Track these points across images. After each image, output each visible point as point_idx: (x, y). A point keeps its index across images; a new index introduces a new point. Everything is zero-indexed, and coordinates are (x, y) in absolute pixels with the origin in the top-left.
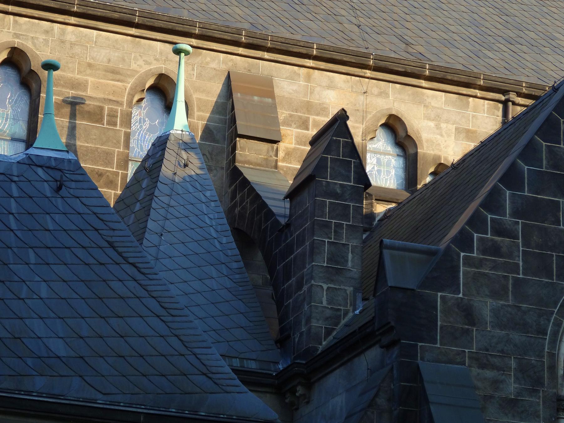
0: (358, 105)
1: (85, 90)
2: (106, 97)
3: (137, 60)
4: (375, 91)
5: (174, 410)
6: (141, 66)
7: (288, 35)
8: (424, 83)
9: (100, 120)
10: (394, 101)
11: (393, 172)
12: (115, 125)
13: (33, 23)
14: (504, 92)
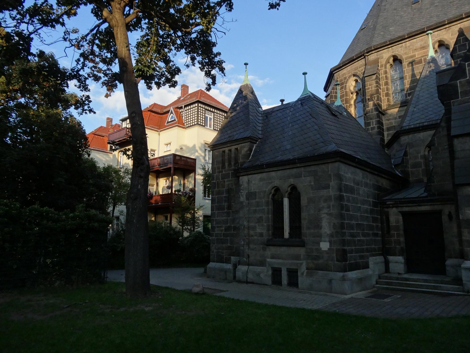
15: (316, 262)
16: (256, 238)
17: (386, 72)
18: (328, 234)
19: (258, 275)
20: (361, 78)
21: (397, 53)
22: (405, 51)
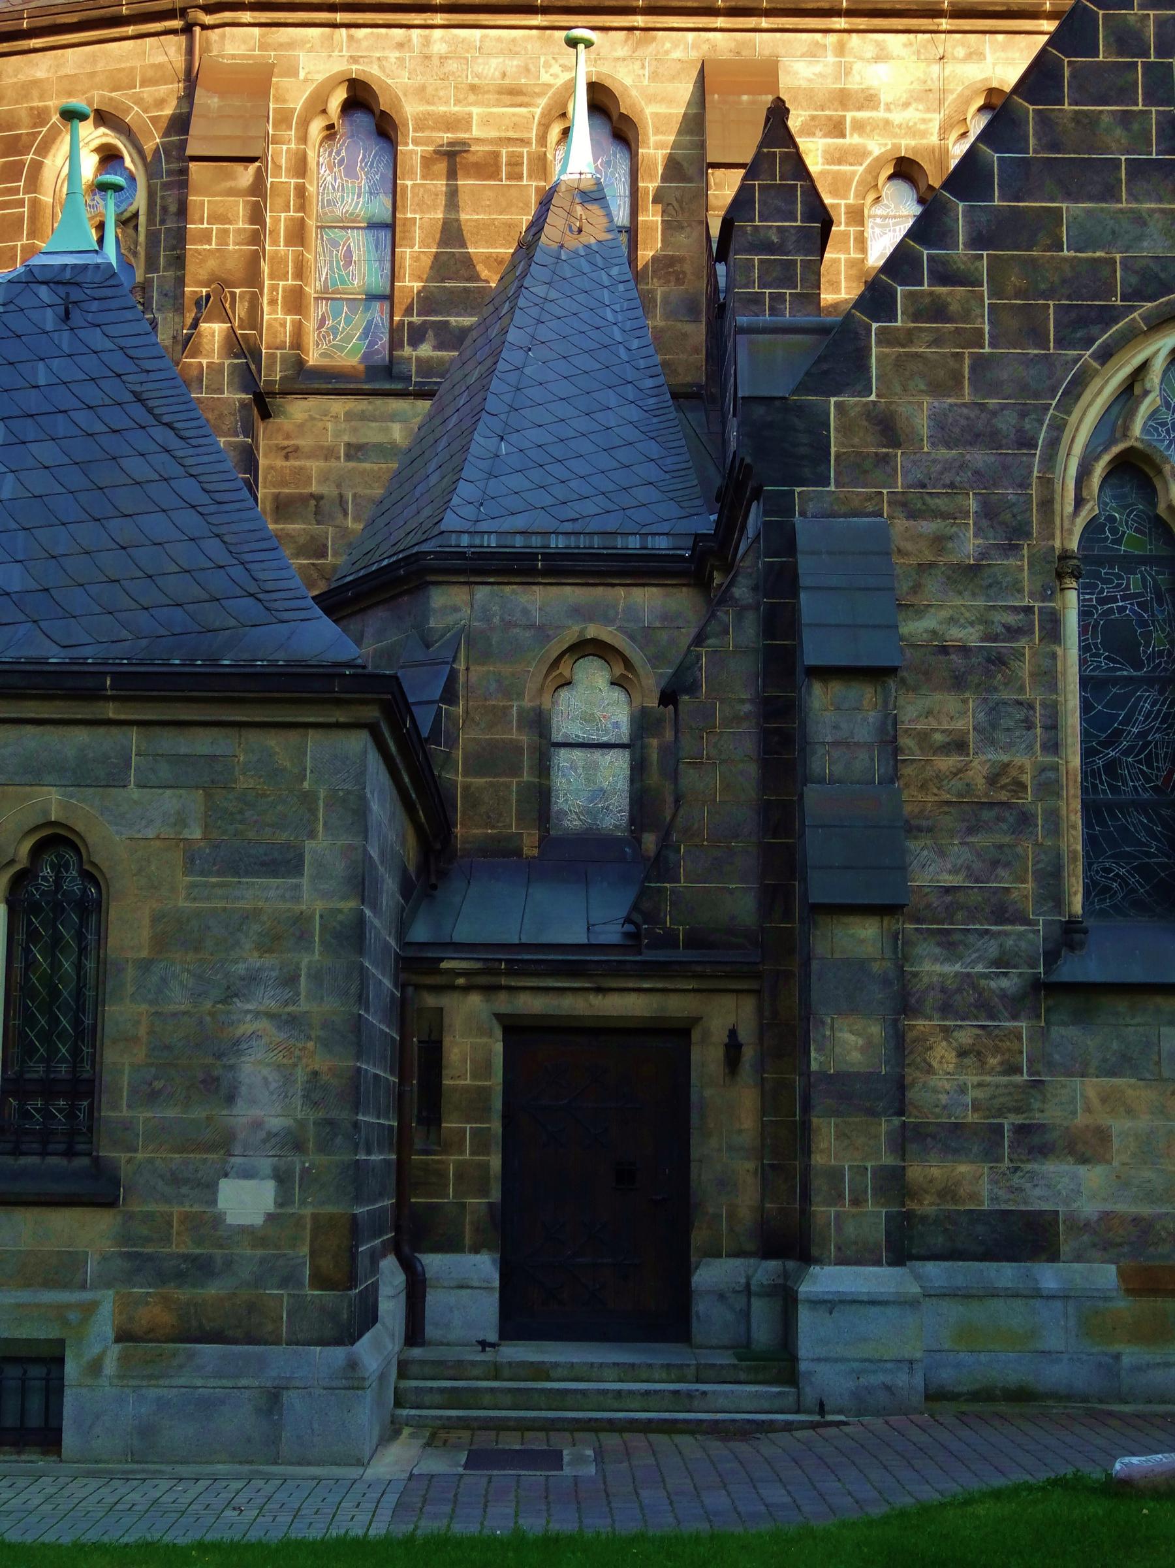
0: (929, 82)
1: (469, 128)
2: (503, 135)
3: (550, 66)
4: (960, 52)
5: (177, 662)
6: (555, 76)
9: (495, 174)
10: (994, 65)
12: (520, 178)
13: (379, 36)
15: (183, 1294)
17: (301, 167)
18: (271, 1135)
20: (149, 147)
21: (375, 70)
22: (420, 80)
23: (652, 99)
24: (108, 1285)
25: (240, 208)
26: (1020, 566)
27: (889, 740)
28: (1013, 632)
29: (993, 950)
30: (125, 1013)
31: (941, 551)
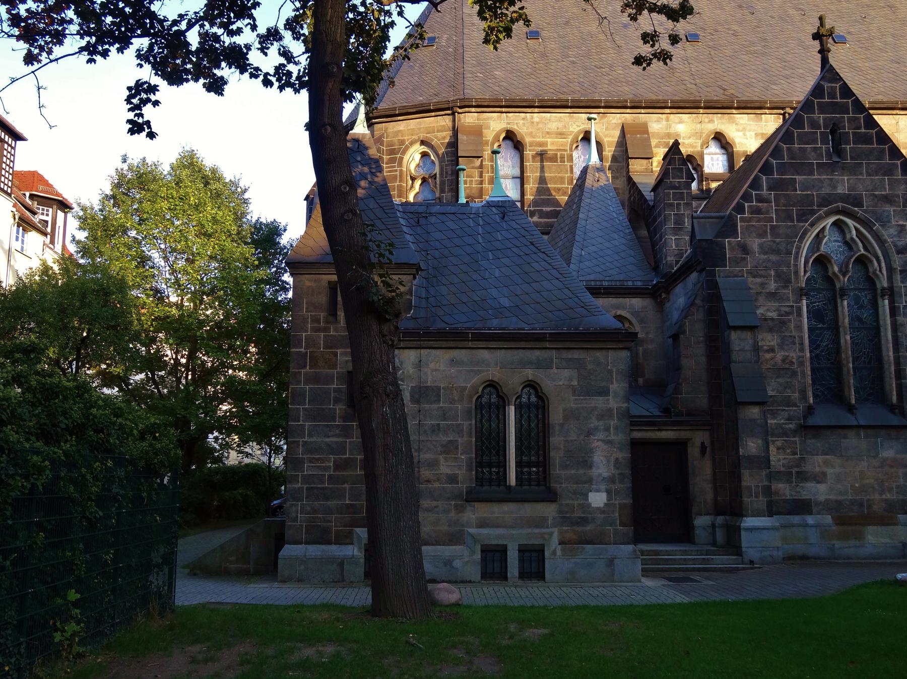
4: (706, 120)
7: (654, 97)
8: (734, 111)
9: (556, 161)
11: (721, 164)
14: (783, 108)
15: (580, 529)
16: (437, 485)
19: (448, 563)
20: (440, 152)
21: (515, 127)
22: (530, 130)
23: (606, 136)
24: (555, 527)
25: (476, 173)
26: (789, 292)
27: (756, 348)
28: (788, 314)
29: (786, 414)
30: (556, 440)
31: (763, 288)
